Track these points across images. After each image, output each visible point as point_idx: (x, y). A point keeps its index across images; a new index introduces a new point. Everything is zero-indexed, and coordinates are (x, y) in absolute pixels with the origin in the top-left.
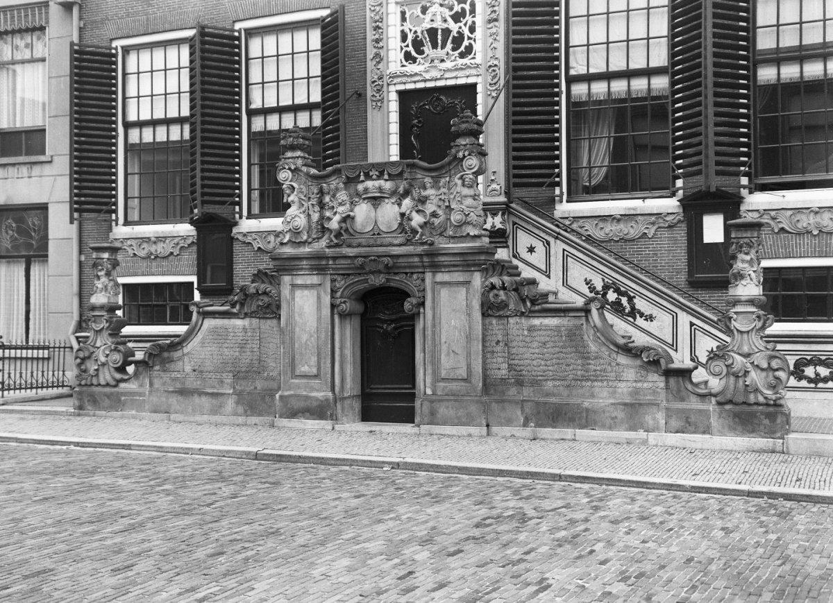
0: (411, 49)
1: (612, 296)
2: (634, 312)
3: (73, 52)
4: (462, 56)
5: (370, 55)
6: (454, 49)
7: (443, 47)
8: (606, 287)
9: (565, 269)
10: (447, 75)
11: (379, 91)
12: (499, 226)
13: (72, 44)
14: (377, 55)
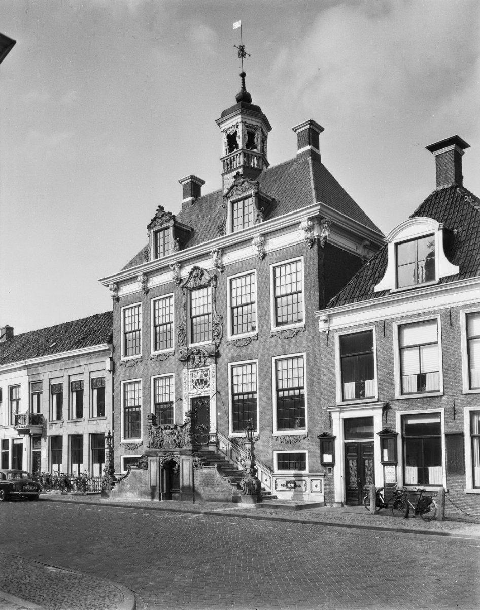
0: (194, 385)
4: (207, 387)
6: (205, 385)
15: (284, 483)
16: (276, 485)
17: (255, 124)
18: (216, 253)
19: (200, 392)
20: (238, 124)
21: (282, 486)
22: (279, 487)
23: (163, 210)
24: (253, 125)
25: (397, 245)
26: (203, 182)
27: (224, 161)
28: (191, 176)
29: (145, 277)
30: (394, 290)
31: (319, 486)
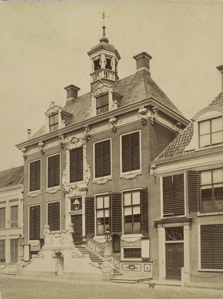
7: (77, 207)
8: (101, 252)
10: (78, 213)
12: (85, 241)
15: (128, 266)
16: (123, 267)
17: (111, 55)
18: (87, 128)
19: (76, 212)
20: (100, 55)
21: (127, 268)
22: (125, 269)
23: (54, 104)
24: (109, 55)
25: (199, 123)
26: (79, 89)
27: (92, 76)
29: (43, 144)
30: (197, 149)
31: (149, 268)
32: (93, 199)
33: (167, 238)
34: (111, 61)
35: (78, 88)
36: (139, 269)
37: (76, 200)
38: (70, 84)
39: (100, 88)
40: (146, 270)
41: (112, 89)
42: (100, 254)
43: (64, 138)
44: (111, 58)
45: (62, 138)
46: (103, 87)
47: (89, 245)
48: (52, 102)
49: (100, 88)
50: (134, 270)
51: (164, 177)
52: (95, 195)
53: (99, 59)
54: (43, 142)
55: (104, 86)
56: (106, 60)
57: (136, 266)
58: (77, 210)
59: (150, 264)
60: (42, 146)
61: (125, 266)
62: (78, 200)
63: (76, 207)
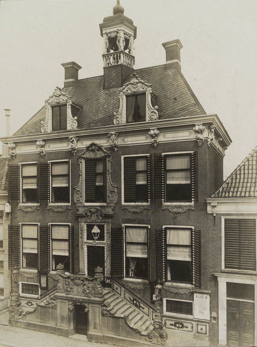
1: (135, 302)
2: (140, 306)
3: (9, 227)
5: (80, 236)
7: (97, 237)
8: (134, 300)
9: (125, 294)
11: (82, 245)
13: (9, 225)
14: (81, 237)
15: (173, 323)
17: (130, 33)
18: (114, 135)
19: (97, 243)
20: (118, 31)
21: (171, 325)
24: (128, 33)
26: (80, 68)
28: (73, 62)
32: (120, 229)
33: (228, 295)
34: (130, 42)
35: (80, 66)
36: (190, 329)
37: (95, 227)
38: (71, 61)
39: (132, 84)
40: (199, 330)
41: (151, 89)
42: (132, 302)
43: (77, 141)
44: (129, 37)
45: (75, 141)
46: (137, 83)
47: (115, 288)
48: (57, 88)
49: (132, 84)
50: (182, 329)
51: (225, 218)
52: (123, 225)
53: (116, 37)
54: (44, 140)
55: (141, 82)
56: (124, 40)
57: (185, 324)
58: (97, 240)
59: (206, 325)
60: (42, 146)
61: (168, 323)
62: (97, 228)
63: (95, 236)
